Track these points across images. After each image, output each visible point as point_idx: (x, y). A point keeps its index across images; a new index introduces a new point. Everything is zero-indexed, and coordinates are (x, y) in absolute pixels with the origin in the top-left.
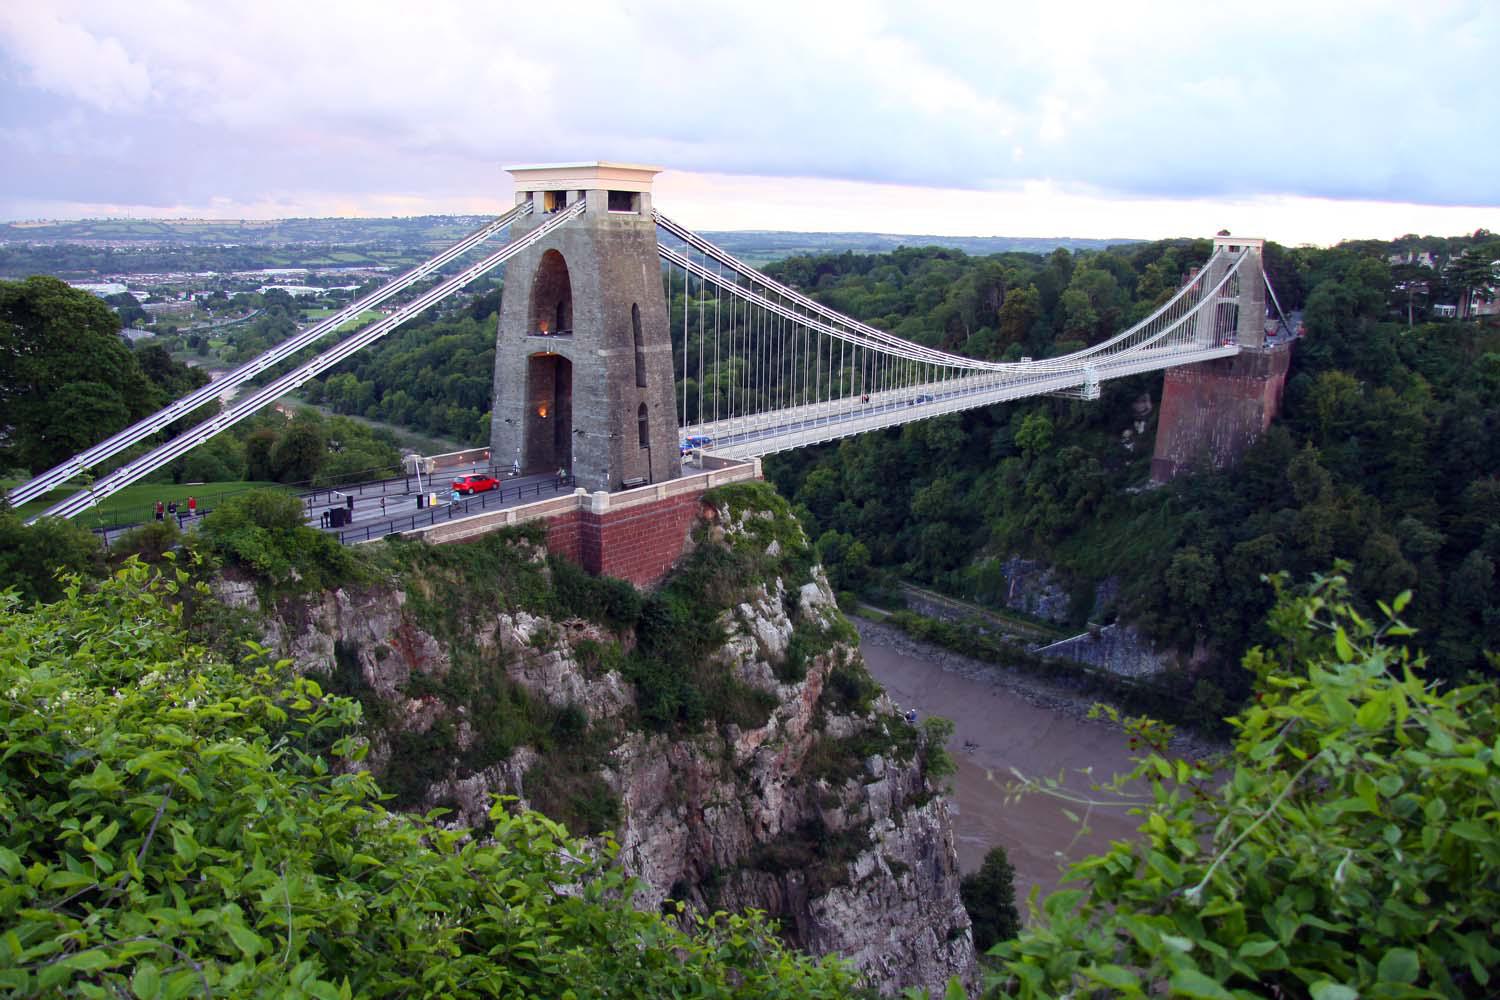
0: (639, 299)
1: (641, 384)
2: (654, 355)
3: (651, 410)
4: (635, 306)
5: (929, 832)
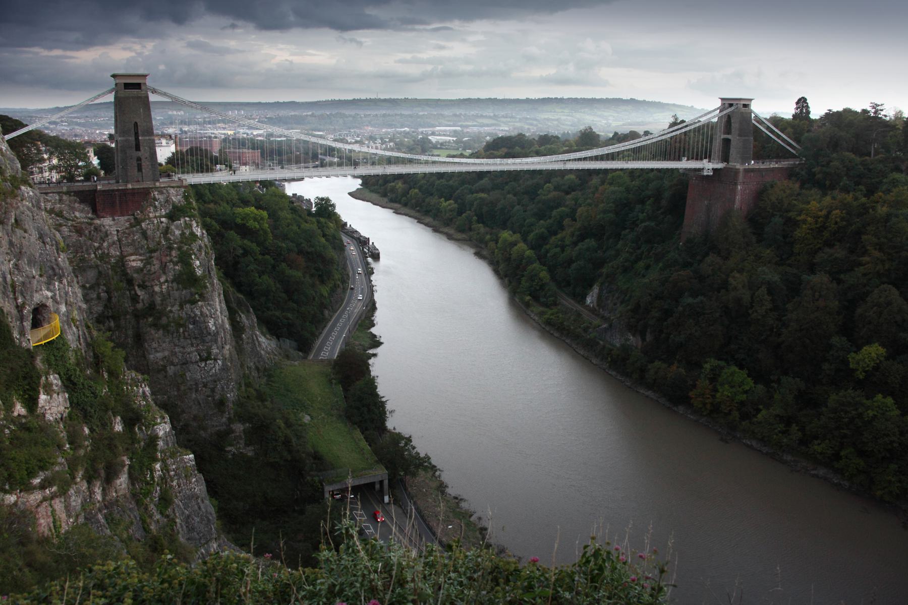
0: (138, 121)
1: (138, 148)
2: (145, 140)
3: (143, 160)
4: (136, 124)
5: (196, 315)
